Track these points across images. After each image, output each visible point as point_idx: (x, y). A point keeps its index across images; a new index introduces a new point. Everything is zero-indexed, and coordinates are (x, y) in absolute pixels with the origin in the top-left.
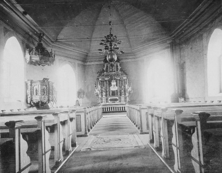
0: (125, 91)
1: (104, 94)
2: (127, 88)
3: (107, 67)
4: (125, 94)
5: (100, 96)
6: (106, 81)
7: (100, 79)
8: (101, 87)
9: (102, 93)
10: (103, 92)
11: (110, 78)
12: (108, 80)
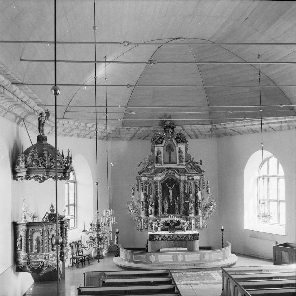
0: (196, 206)
1: (151, 209)
2: (200, 198)
3: (159, 153)
4: (197, 213)
5: (143, 215)
6: (156, 183)
7: (143, 179)
8: (145, 195)
9: (147, 208)
10: (150, 207)
12: (160, 181)
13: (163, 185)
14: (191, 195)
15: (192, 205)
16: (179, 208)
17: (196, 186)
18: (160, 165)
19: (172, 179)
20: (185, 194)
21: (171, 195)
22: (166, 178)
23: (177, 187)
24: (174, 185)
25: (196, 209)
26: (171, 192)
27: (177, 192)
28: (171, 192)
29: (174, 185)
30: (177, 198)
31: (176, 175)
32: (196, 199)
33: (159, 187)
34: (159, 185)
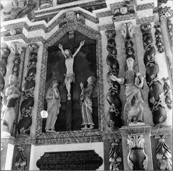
11: (57, 28)
12: (45, 42)
13: (53, 51)
14: (131, 63)
15: (136, 91)
16: (95, 107)
17: (146, 36)
18: (46, 7)
19: (76, 33)
20: (112, 60)
21: (70, 70)
22: (62, 34)
23: (91, 46)
24: (81, 45)
25: (151, 105)
26: (69, 63)
27: (88, 62)
28: (69, 63)
29: (81, 45)
30: (89, 80)
31: (89, 23)
32: (151, 68)
33: (40, 57)
34: (41, 53)
